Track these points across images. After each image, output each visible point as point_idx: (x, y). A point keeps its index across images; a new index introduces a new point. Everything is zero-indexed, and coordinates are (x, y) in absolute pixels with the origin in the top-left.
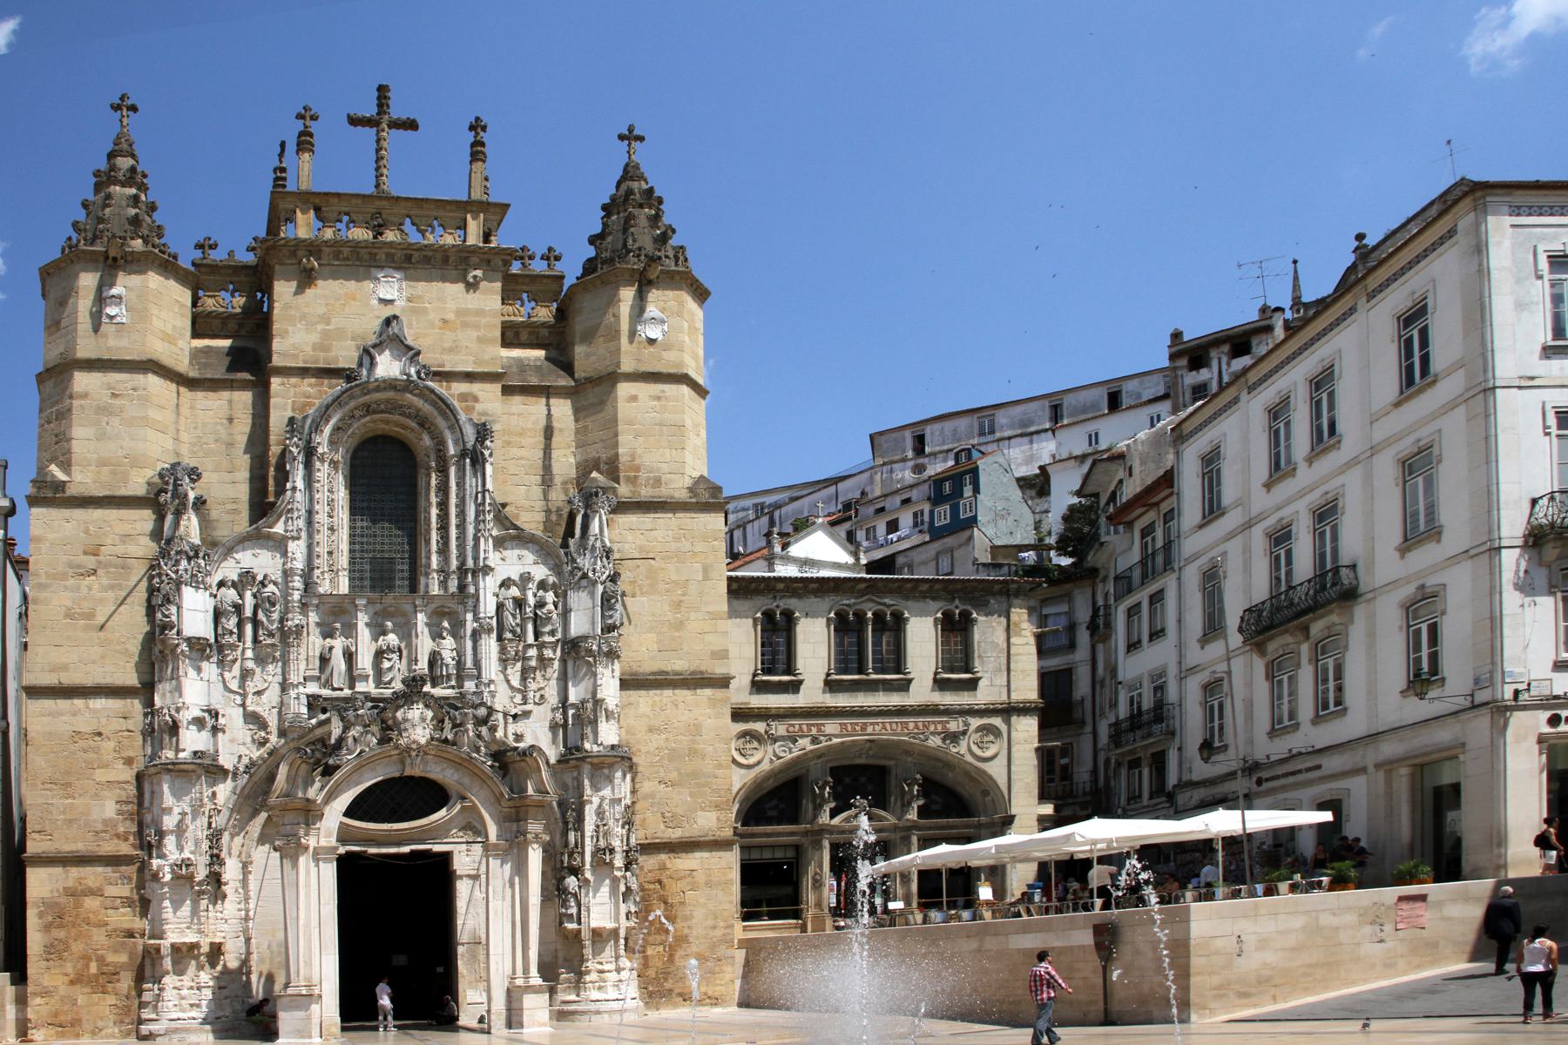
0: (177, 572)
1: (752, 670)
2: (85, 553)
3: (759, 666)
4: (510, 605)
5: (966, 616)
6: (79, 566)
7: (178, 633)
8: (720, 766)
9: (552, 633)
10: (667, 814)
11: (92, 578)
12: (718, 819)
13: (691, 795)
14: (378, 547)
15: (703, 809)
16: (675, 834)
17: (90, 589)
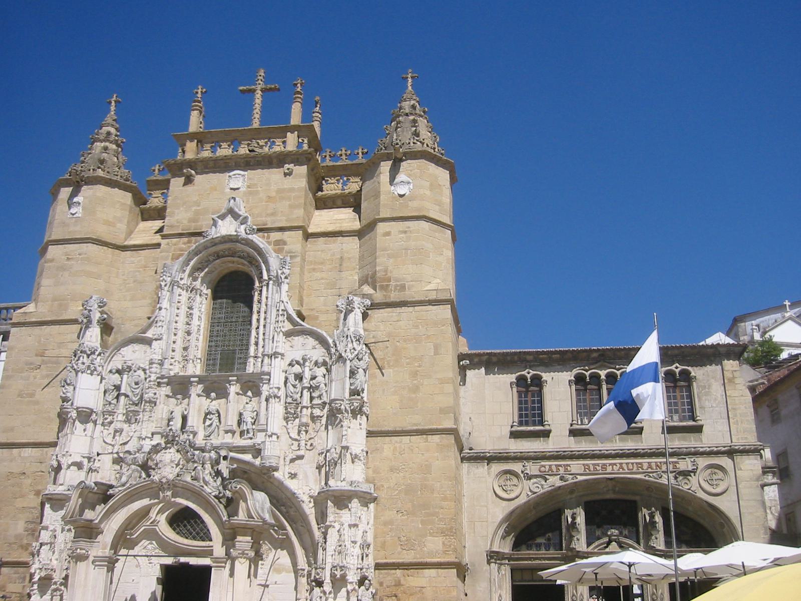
0: (77, 365)
1: (511, 423)
2: (37, 355)
3: (516, 419)
4: (292, 378)
5: (686, 375)
6: (31, 364)
7: (72, 404)
8: (445, 499)
9: (320, 397)
10: (403, 539)
11: (38, 371)
12: (443, 543)
13: (422, 522)
14: (227, 343)
15: (431, 535)
16: (408, 557)
17: (35, 378)
